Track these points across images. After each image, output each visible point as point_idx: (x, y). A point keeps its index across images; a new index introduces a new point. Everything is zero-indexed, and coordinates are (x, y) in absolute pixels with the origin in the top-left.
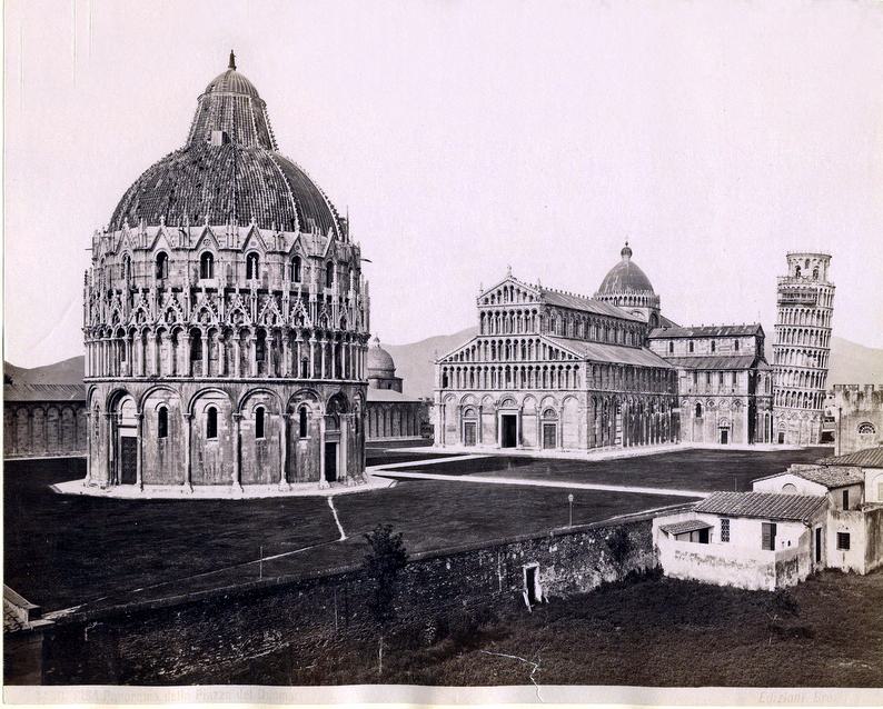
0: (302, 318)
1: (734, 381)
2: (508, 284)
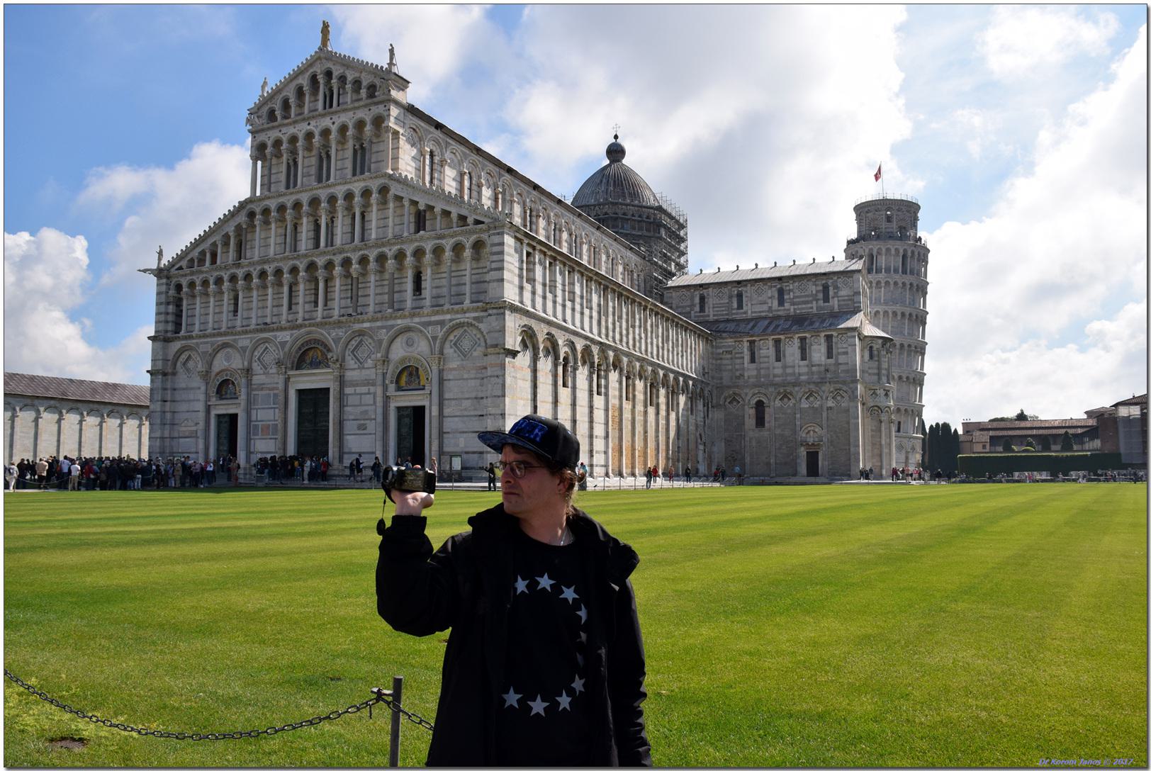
1: (830, 356)
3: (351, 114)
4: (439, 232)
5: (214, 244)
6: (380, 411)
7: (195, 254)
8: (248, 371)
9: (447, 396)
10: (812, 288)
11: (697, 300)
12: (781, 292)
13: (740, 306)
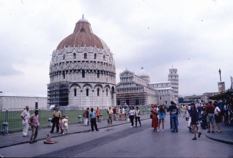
0: (106, 69)
2: (126, 71)
10: (166, 84)
12: (162, 85)
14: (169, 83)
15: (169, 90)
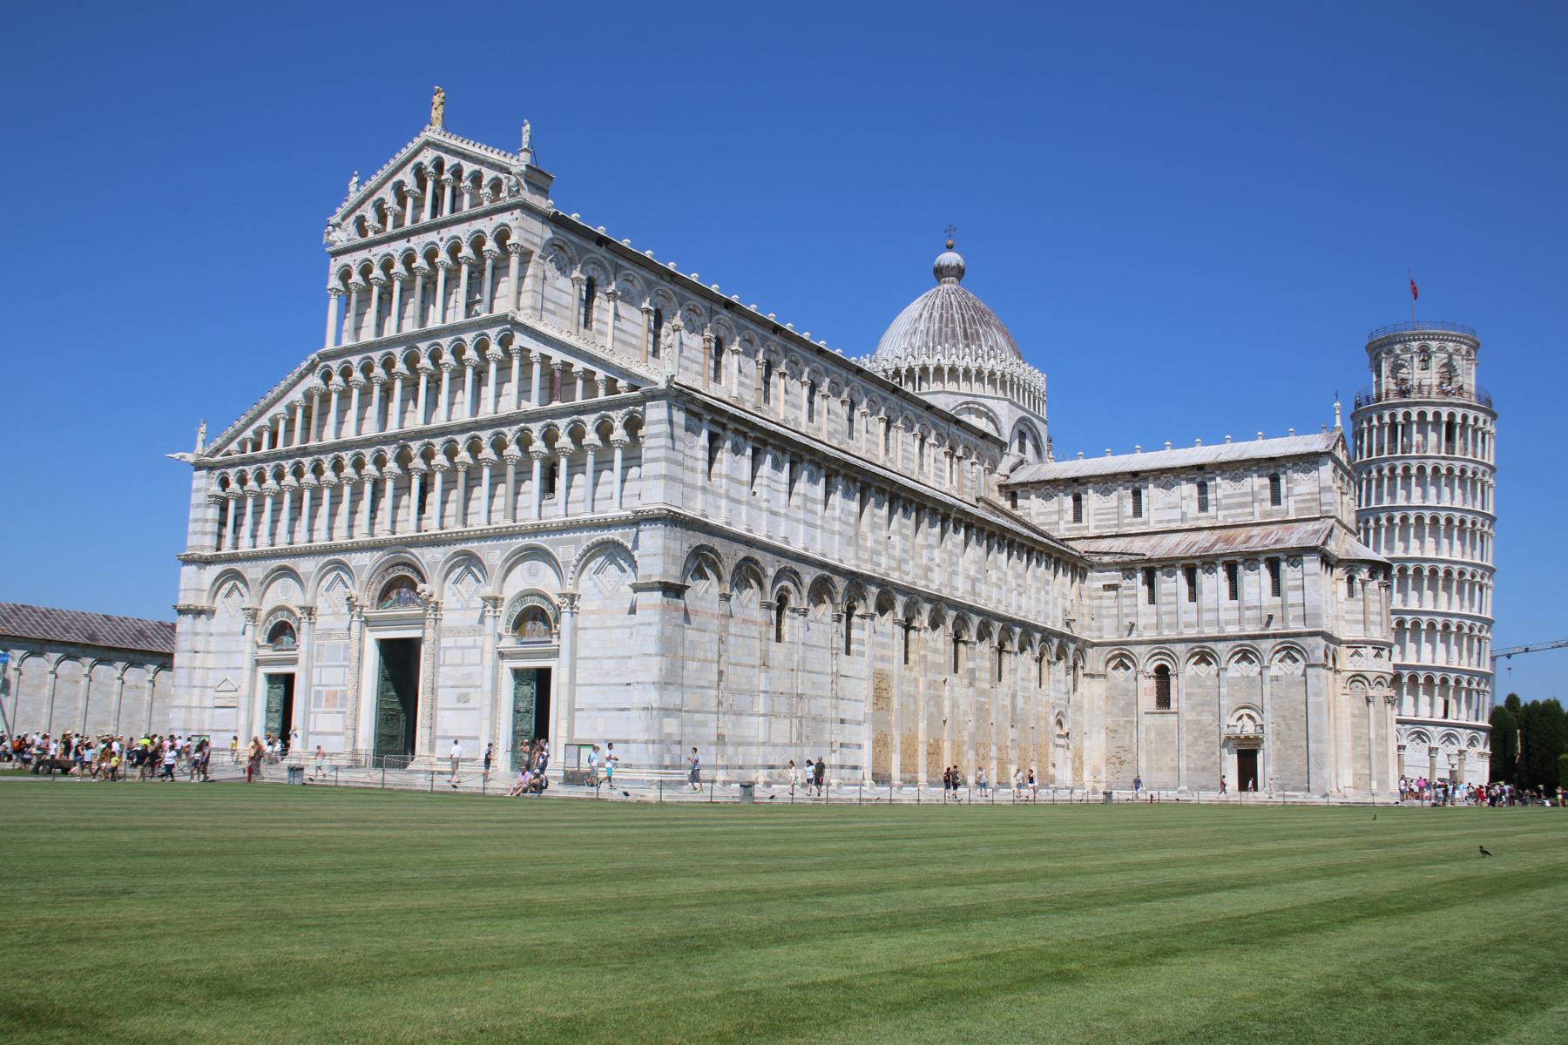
1: (1277, 590)
3: (465, 226)
4: (579, 400)
5: (275, 421)
6: (488, 673)
7: (249, 433)
8: (310, 611)
9: (581, 653)
11: (1069, 502)
13: (1138, 512)
14: (1308, 461)
15: (1296, 555)
